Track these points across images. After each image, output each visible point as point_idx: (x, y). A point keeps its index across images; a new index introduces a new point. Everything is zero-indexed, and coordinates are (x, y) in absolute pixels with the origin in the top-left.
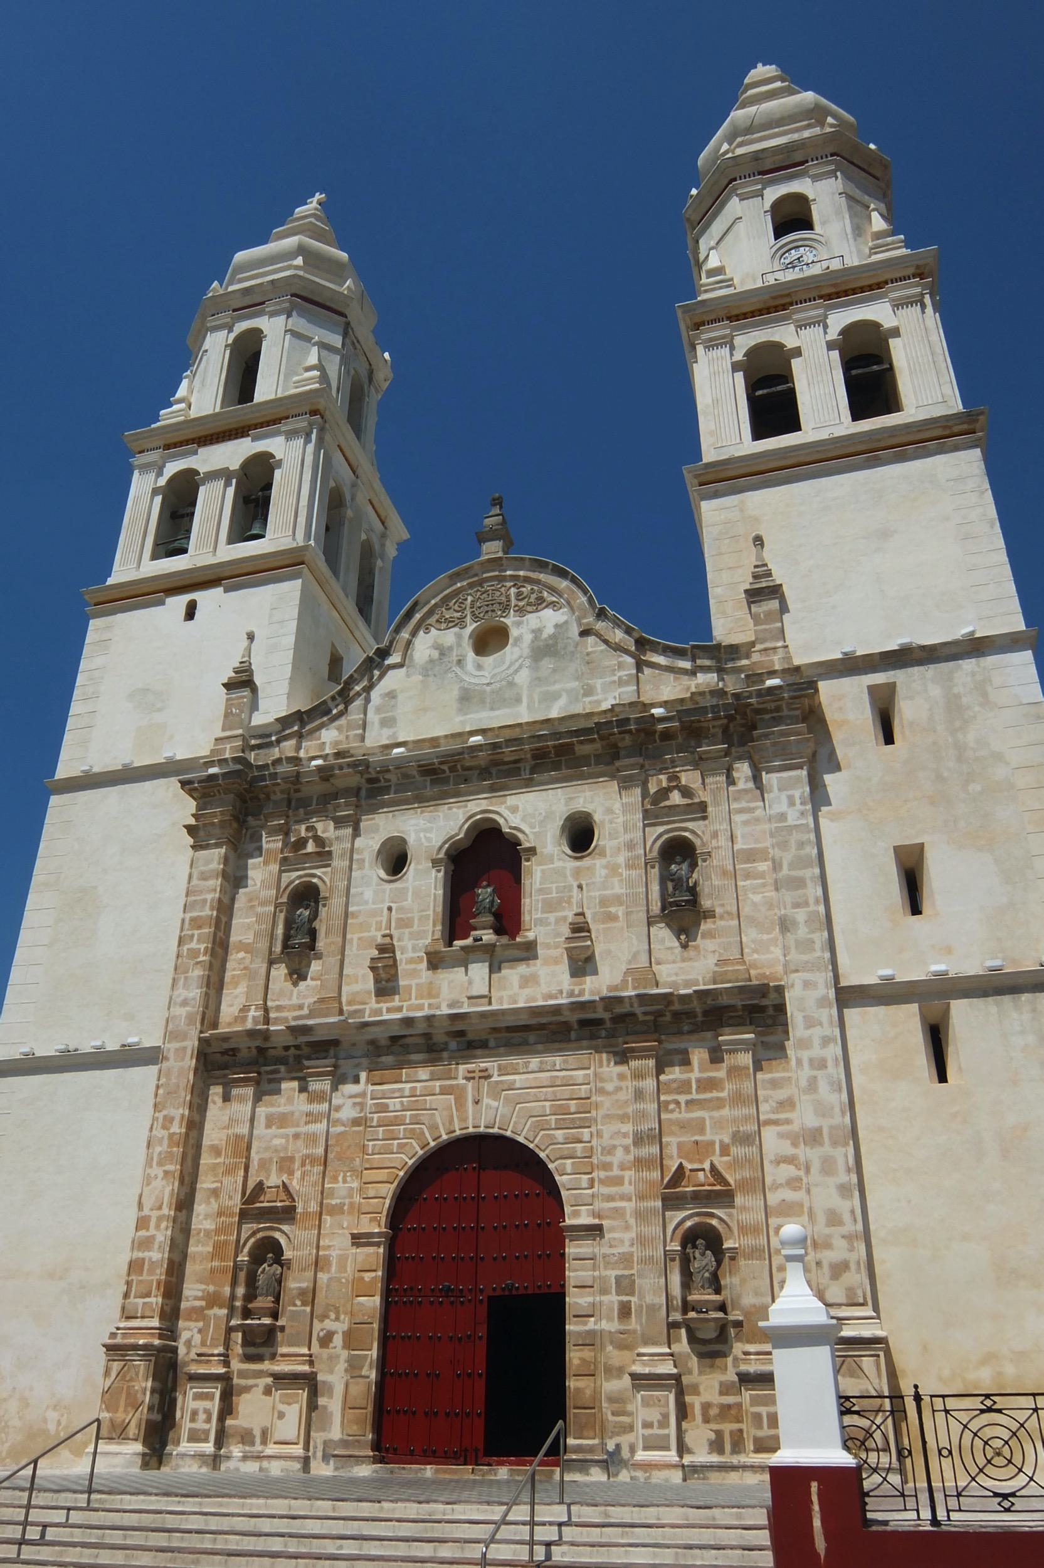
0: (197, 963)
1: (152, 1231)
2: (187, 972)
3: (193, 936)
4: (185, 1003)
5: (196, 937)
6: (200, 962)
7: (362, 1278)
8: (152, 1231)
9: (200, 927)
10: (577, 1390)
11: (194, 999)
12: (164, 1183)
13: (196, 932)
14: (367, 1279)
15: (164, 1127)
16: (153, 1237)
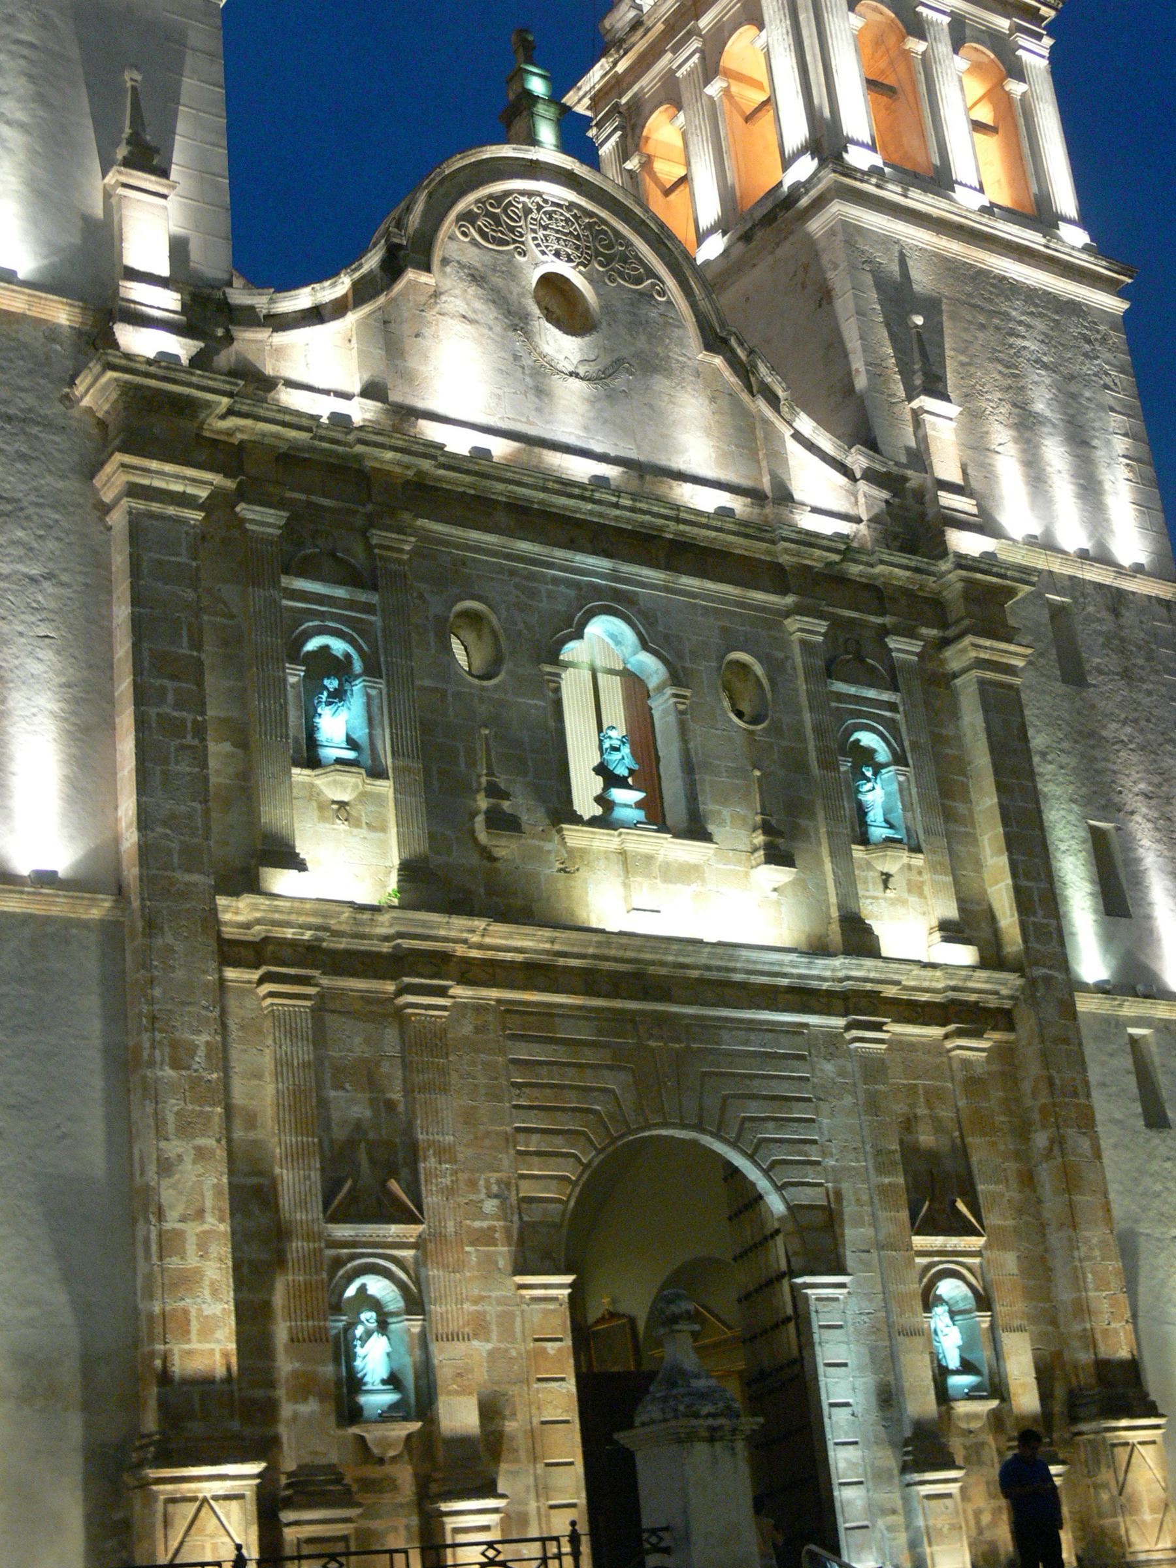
0: (182, 747)
1: (192, 1261)
2: (166, 761)
3: (163, 690)
4: (170, 821)
5: (170, 698)
6: (190, 747)
7: (545, 1349)
8: (193, 1260)
9: (173, 677)
10: (849, 1502)
11: (190, 816)
12: (199, 1169)
13: (168, 684)
14: (551, 1352)
15: (176, 1065)
16: (198, 1274)
